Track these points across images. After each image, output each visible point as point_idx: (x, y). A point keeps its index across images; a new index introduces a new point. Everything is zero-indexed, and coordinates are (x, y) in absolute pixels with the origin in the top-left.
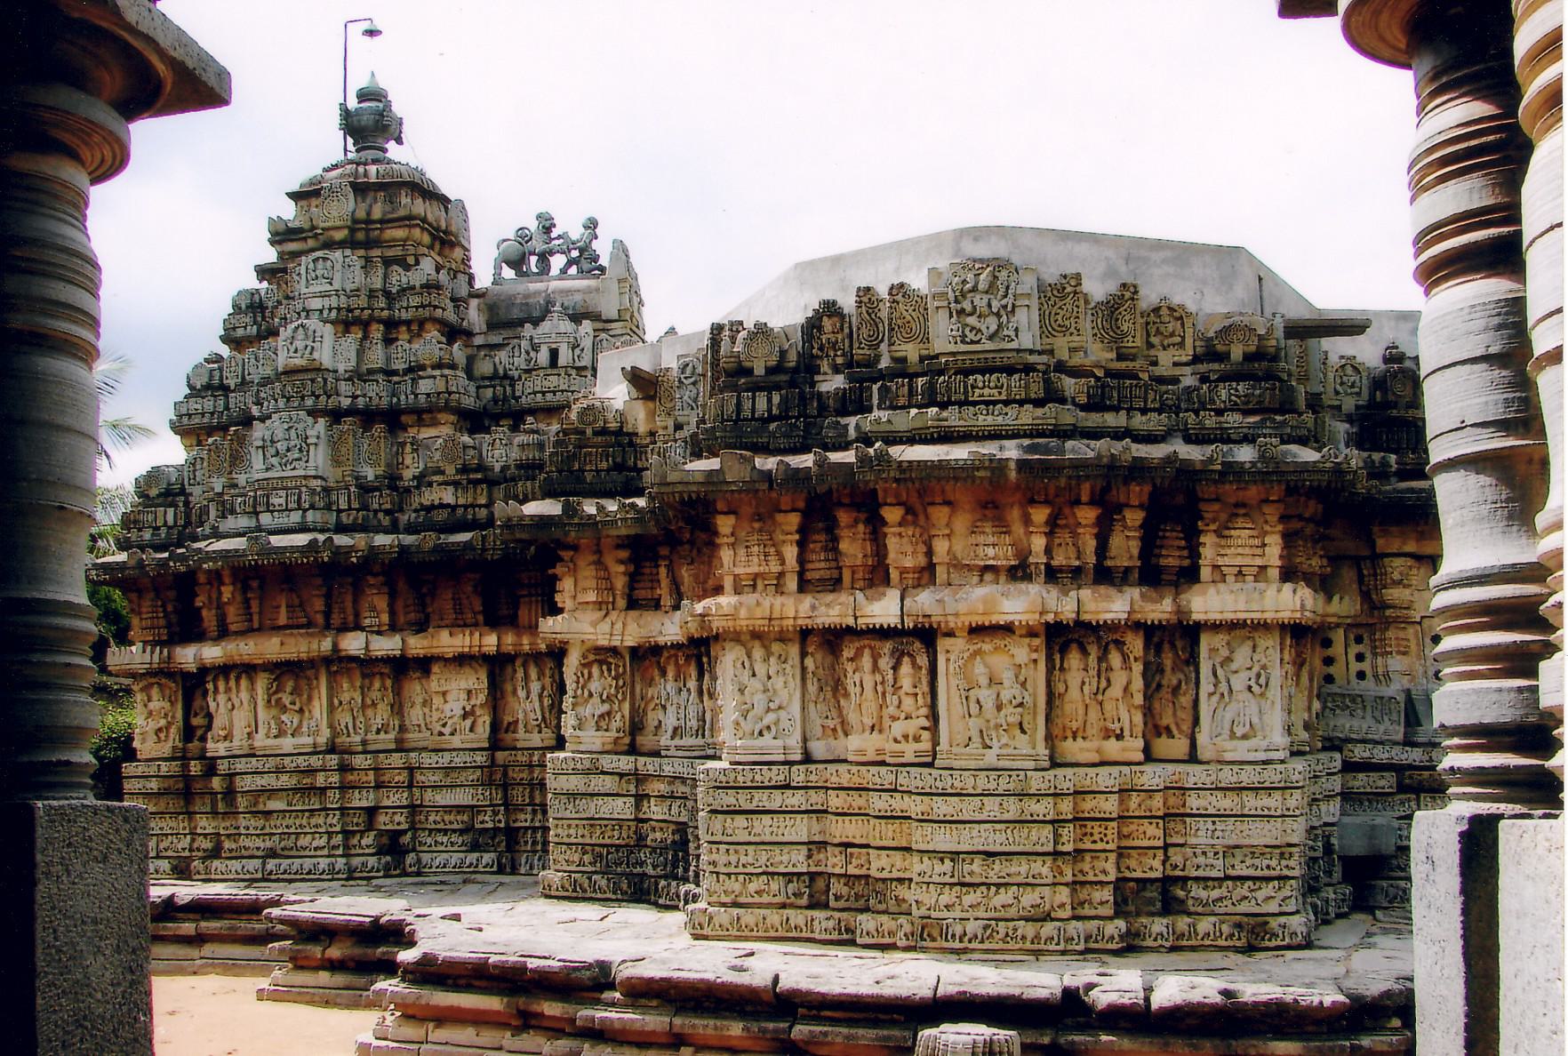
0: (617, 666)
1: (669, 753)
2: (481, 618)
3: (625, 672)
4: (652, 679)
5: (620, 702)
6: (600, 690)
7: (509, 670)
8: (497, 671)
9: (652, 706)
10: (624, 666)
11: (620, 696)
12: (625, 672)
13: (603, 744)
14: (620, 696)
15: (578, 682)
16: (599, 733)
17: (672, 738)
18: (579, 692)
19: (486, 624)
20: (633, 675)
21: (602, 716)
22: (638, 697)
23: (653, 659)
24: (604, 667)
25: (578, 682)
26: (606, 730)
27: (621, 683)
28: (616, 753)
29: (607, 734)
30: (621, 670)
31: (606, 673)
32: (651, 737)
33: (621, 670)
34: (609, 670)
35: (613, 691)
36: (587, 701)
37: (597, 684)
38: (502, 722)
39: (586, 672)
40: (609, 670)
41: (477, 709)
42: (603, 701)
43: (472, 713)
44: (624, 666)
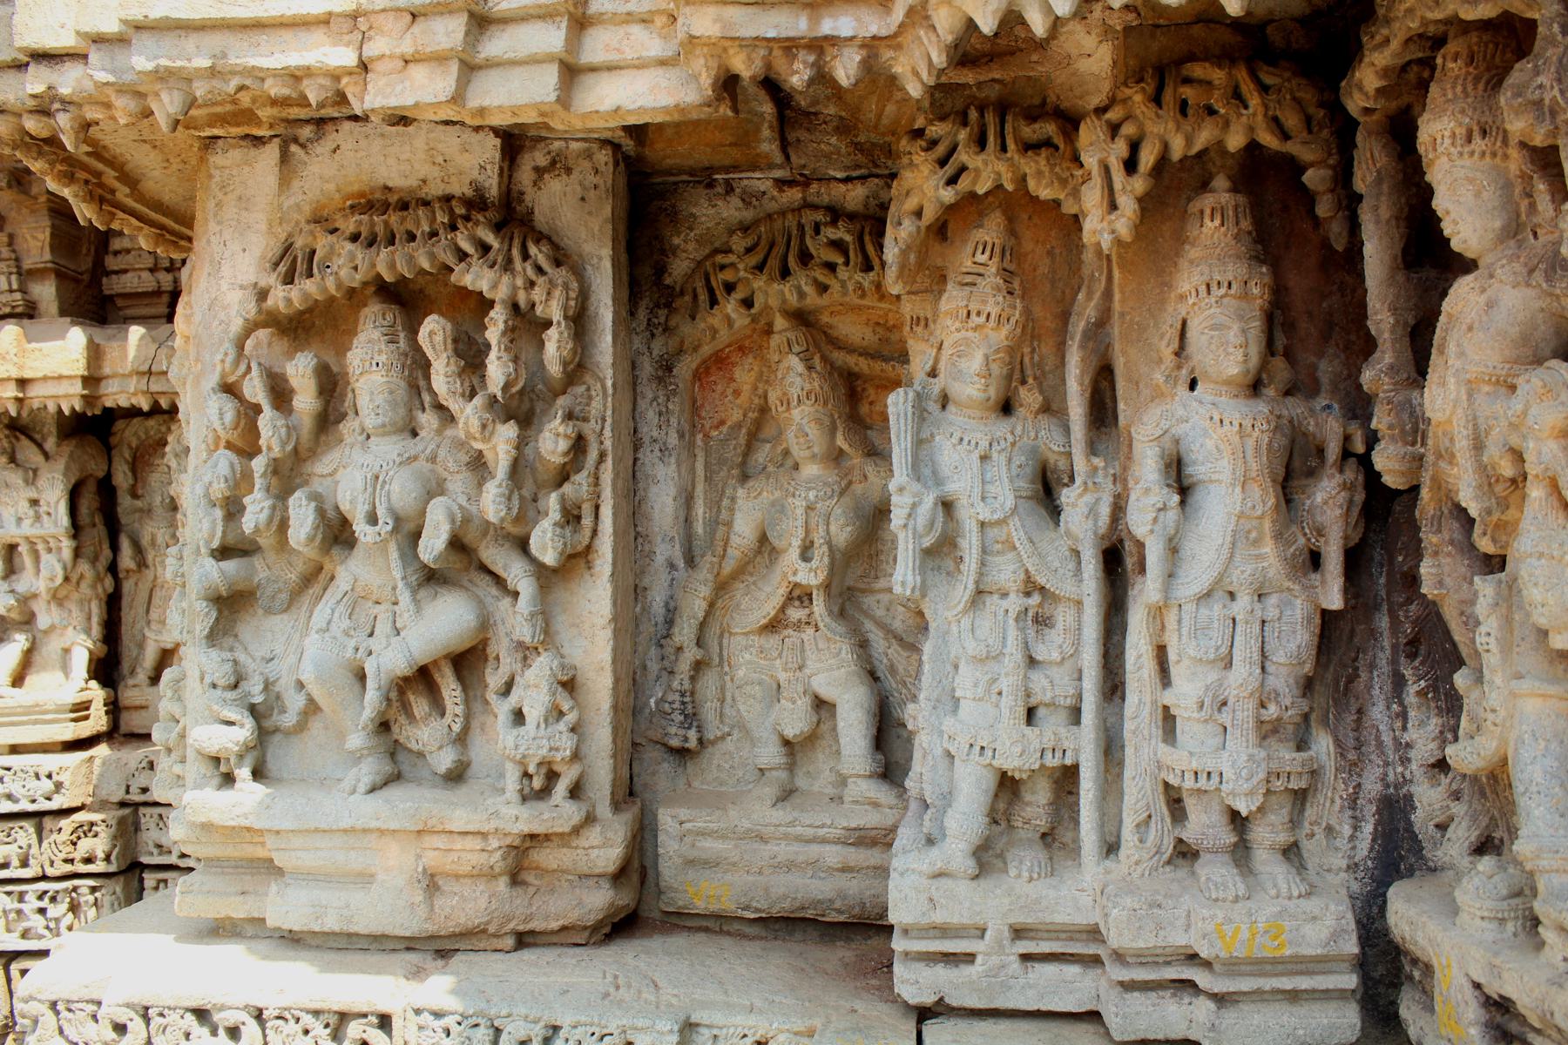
0: (526, 324)
1: (959, 986)
2: (46, 292)
3: (577, 369)
4: (759, 425)
5: (547, 577)
6: (401, 491)
7: (154, 479)
8: (122, 478)
9: (762, 600)
10: (579, 321)
11: (546, 543)
12: (577, 369)
13: (432, 883)
14: (546, 543)
15: (246, 446)
16: (402, 805)
17: (986, 858)
18: (256, 510)
19: (63, 312)
20: (631, 382)
21: (423, 678)
22: (665, 550)
23: (773, 294)
24: (434, 331)
25: (246, 446)
26: (456, 776)
27: (552, 442)
28: (524, 940)
29: (460, 811)
30: (555, 346)
31: (443, 376)
32: (761, 812)
33: (555, 346)
34: (471, 357)
35: (492, 503)
36: (313, 578)
37: (388, 449)
38: (141, 646)
39: (300, 370)
40: (471, 357)
41: (39, 607)
42: (432, 578)
43: (28, 620)
44: (579, 321)
